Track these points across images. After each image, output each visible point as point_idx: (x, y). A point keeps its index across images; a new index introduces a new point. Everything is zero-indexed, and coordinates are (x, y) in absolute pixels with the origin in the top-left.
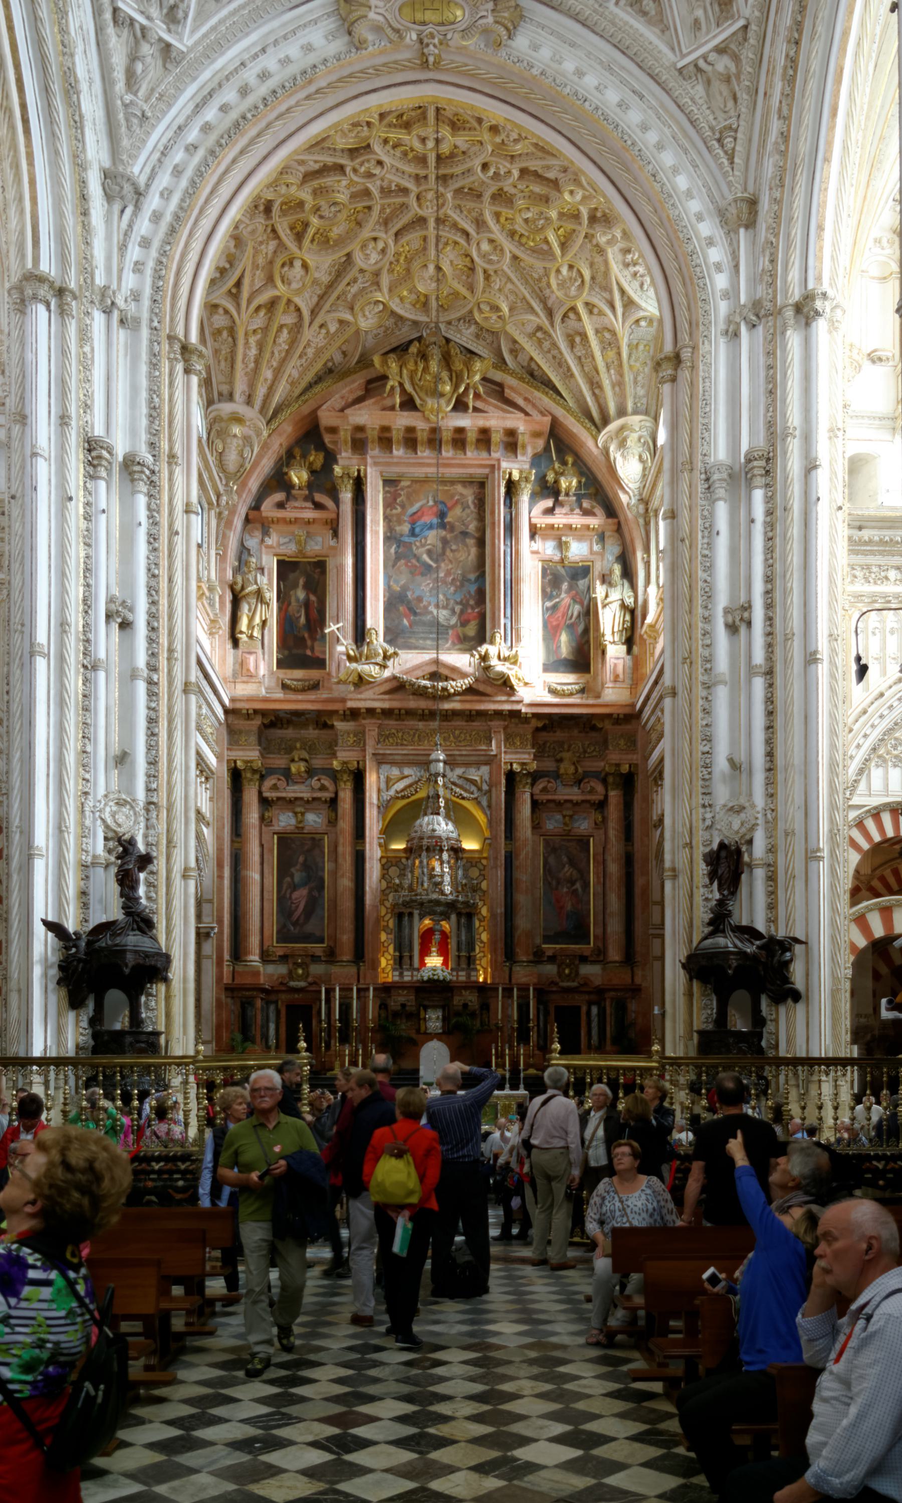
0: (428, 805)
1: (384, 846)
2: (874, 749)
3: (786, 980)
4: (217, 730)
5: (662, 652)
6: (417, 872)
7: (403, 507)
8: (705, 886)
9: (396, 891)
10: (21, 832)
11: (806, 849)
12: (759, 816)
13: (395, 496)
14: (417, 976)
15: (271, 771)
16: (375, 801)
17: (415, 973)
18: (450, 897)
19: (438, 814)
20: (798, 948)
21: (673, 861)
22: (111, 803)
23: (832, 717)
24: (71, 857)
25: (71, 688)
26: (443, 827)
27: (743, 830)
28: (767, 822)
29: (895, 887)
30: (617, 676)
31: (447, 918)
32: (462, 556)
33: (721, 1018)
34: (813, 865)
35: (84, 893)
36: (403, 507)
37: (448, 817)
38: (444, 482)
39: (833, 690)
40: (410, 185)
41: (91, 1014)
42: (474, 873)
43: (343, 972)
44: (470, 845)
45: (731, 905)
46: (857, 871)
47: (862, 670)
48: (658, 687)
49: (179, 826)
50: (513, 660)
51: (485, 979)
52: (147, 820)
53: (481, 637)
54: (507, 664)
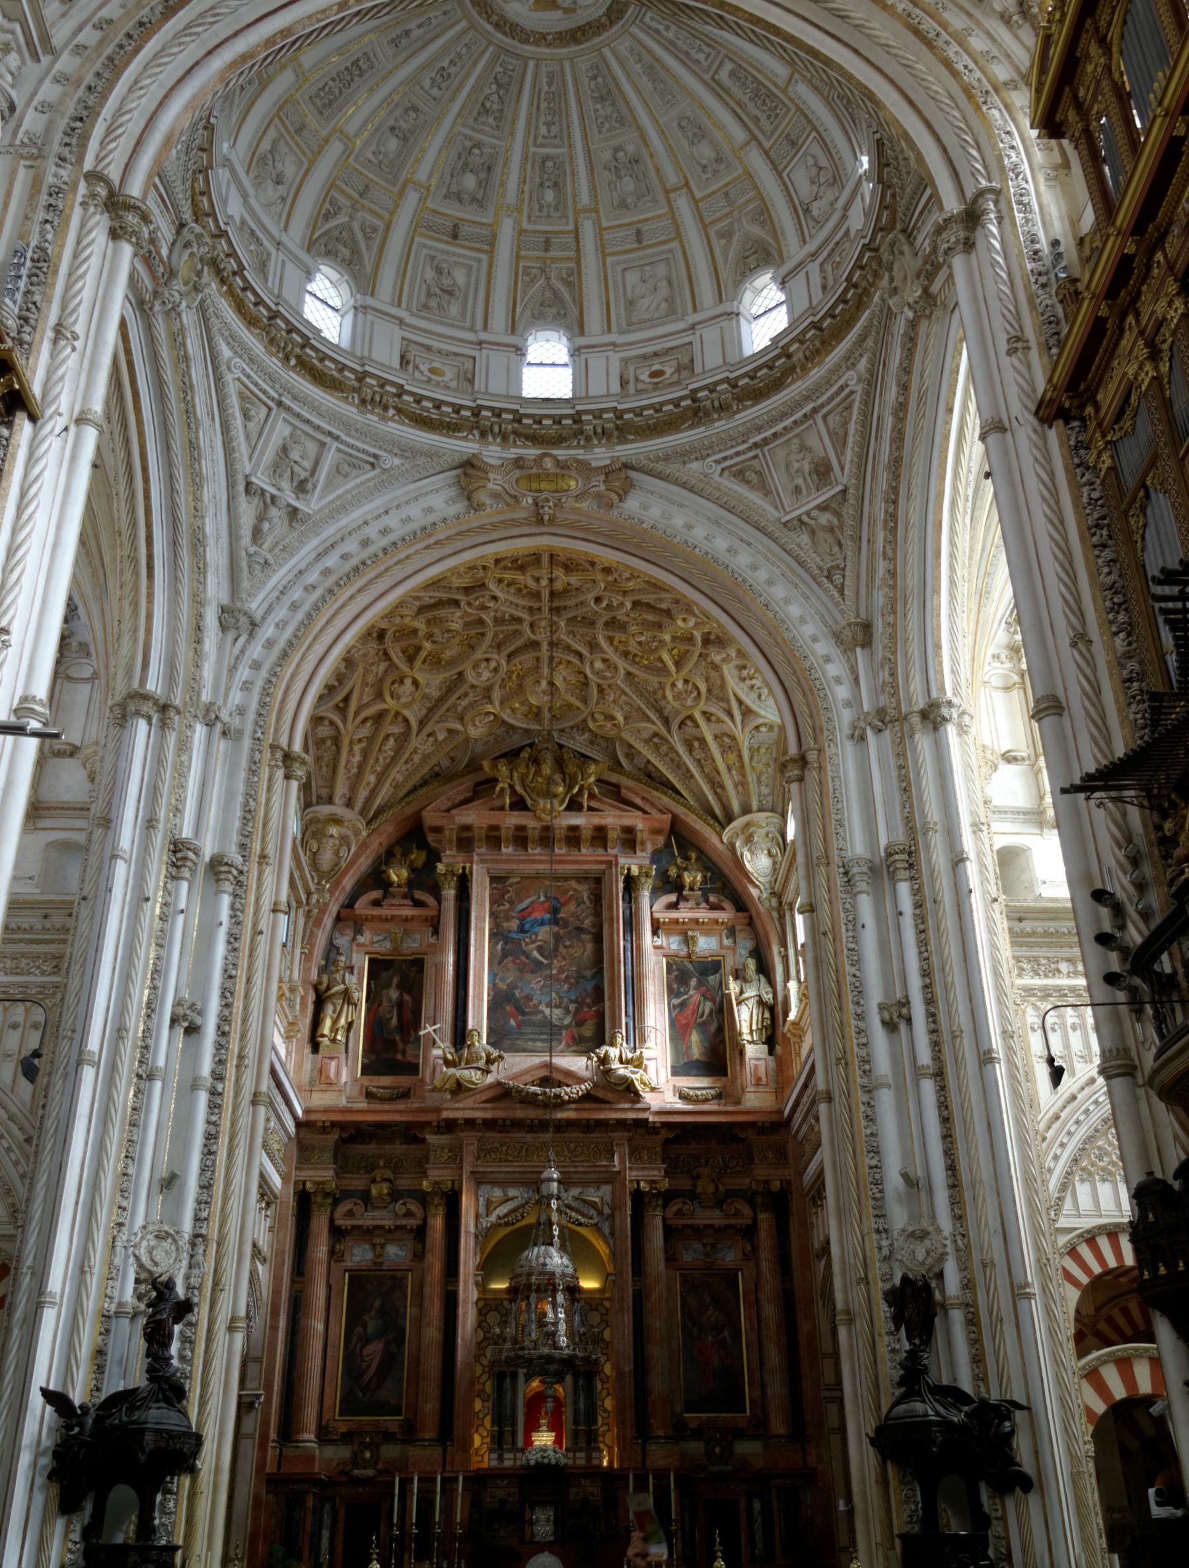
0: (538, 1234)
1: (482, 1286)
2: (1075, 1161)
3: (1010, 1460)
4: (286, 1145)
5: (811, 1050)
6: (523, 1318)
7: (511, 902)
8: (890, 1333)
9: (496, 1344)
10: (33, 1274)
11: (1012, 1284)
12: (948, 1242)
13: (504, 893)
14: (521, 1460)
15: (346, 1194)
16: (472, 1229)
17: (519, 1455)
18: (566, 1351)
19: (551, 1244)
20: (1019, 1415)
21: (846, 1302)
22: (150, 1237)
23: (1019, 1124)
24: (91, 1305)
25: (119, 1100)
26: (557, 1260)
27: (930, 1261)
28: (958, 1250)
29: (1129, 1332)
30: (759, 1079)
31: (561, 1380)
32: (577, 952)
33: (929, 1517)
34: (1022, 1304)
35: (100, 1352)
36: (511, 902)
37: (563, 1248)
38: (557, 879)
39: (1015, 1093)
40: (524, 615)
41: (87, 1520)
42: (595, 1318)
43: (424, 1455)
44: (589, 1284)
45: (926, 1359)
46: (1078, 1312)
47: (1057, 1074)
48: (808, 1092)
49: (230, 1265)
50: (638, 1063)
51: (611, 1462)
52: (192, 1256)
53: (601, 1038)
54: (631, 1068)
